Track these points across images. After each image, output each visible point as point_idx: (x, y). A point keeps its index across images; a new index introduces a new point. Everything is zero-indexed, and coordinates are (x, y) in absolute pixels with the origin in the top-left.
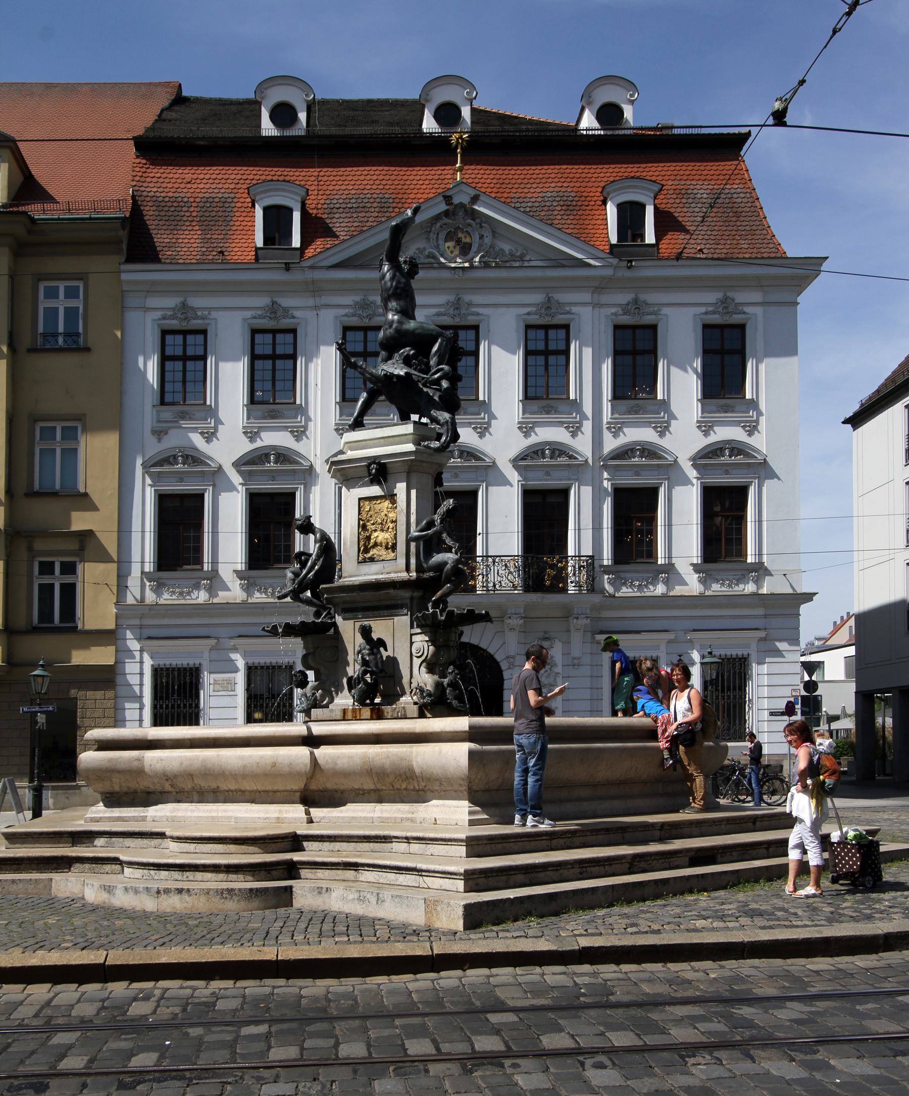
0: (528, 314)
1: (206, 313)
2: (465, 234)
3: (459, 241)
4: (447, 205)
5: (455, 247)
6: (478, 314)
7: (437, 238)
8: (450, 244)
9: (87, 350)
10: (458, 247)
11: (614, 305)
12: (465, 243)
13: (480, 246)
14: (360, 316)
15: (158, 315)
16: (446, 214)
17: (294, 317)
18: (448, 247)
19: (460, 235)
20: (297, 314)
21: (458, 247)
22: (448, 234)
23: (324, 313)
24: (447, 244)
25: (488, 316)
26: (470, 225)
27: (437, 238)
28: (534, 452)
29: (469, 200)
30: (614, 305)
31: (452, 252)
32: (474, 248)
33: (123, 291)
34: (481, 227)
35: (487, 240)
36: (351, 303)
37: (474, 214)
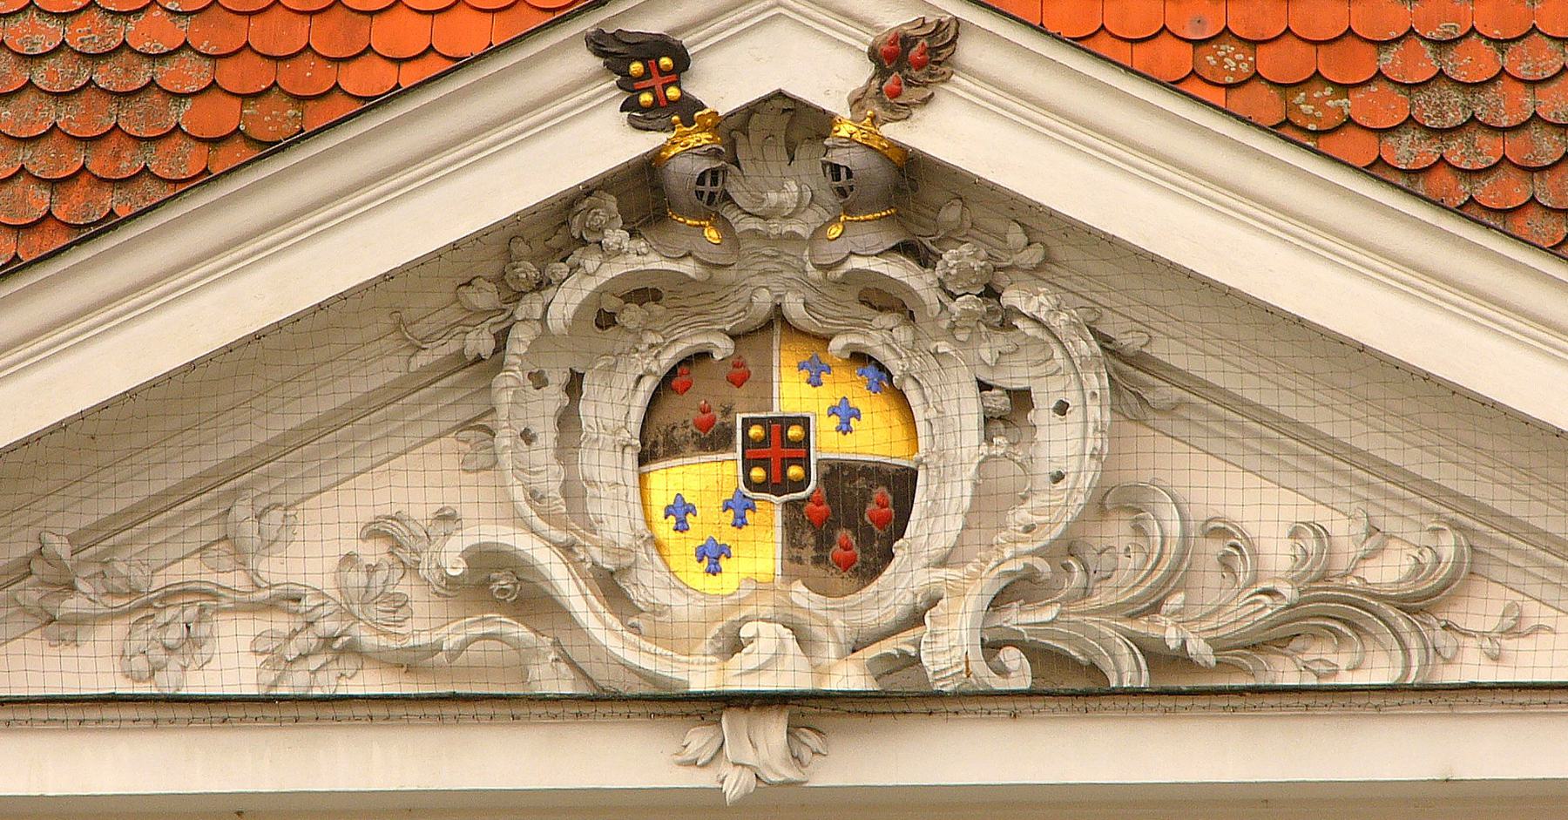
4: (640, 116)
5: (739, 510)
7: (567, 420)
8: (704, 479)
13: (988, 502)
16: (642, 194)
18: (680, 512)
19: (791, 393)
24: (673, 479)
26: (882, 299)
27: (567, 420)
29: (860, 73)
31: (713, 556)
32: (934, 522)
35: (1065, 443)
37: (913, 195)
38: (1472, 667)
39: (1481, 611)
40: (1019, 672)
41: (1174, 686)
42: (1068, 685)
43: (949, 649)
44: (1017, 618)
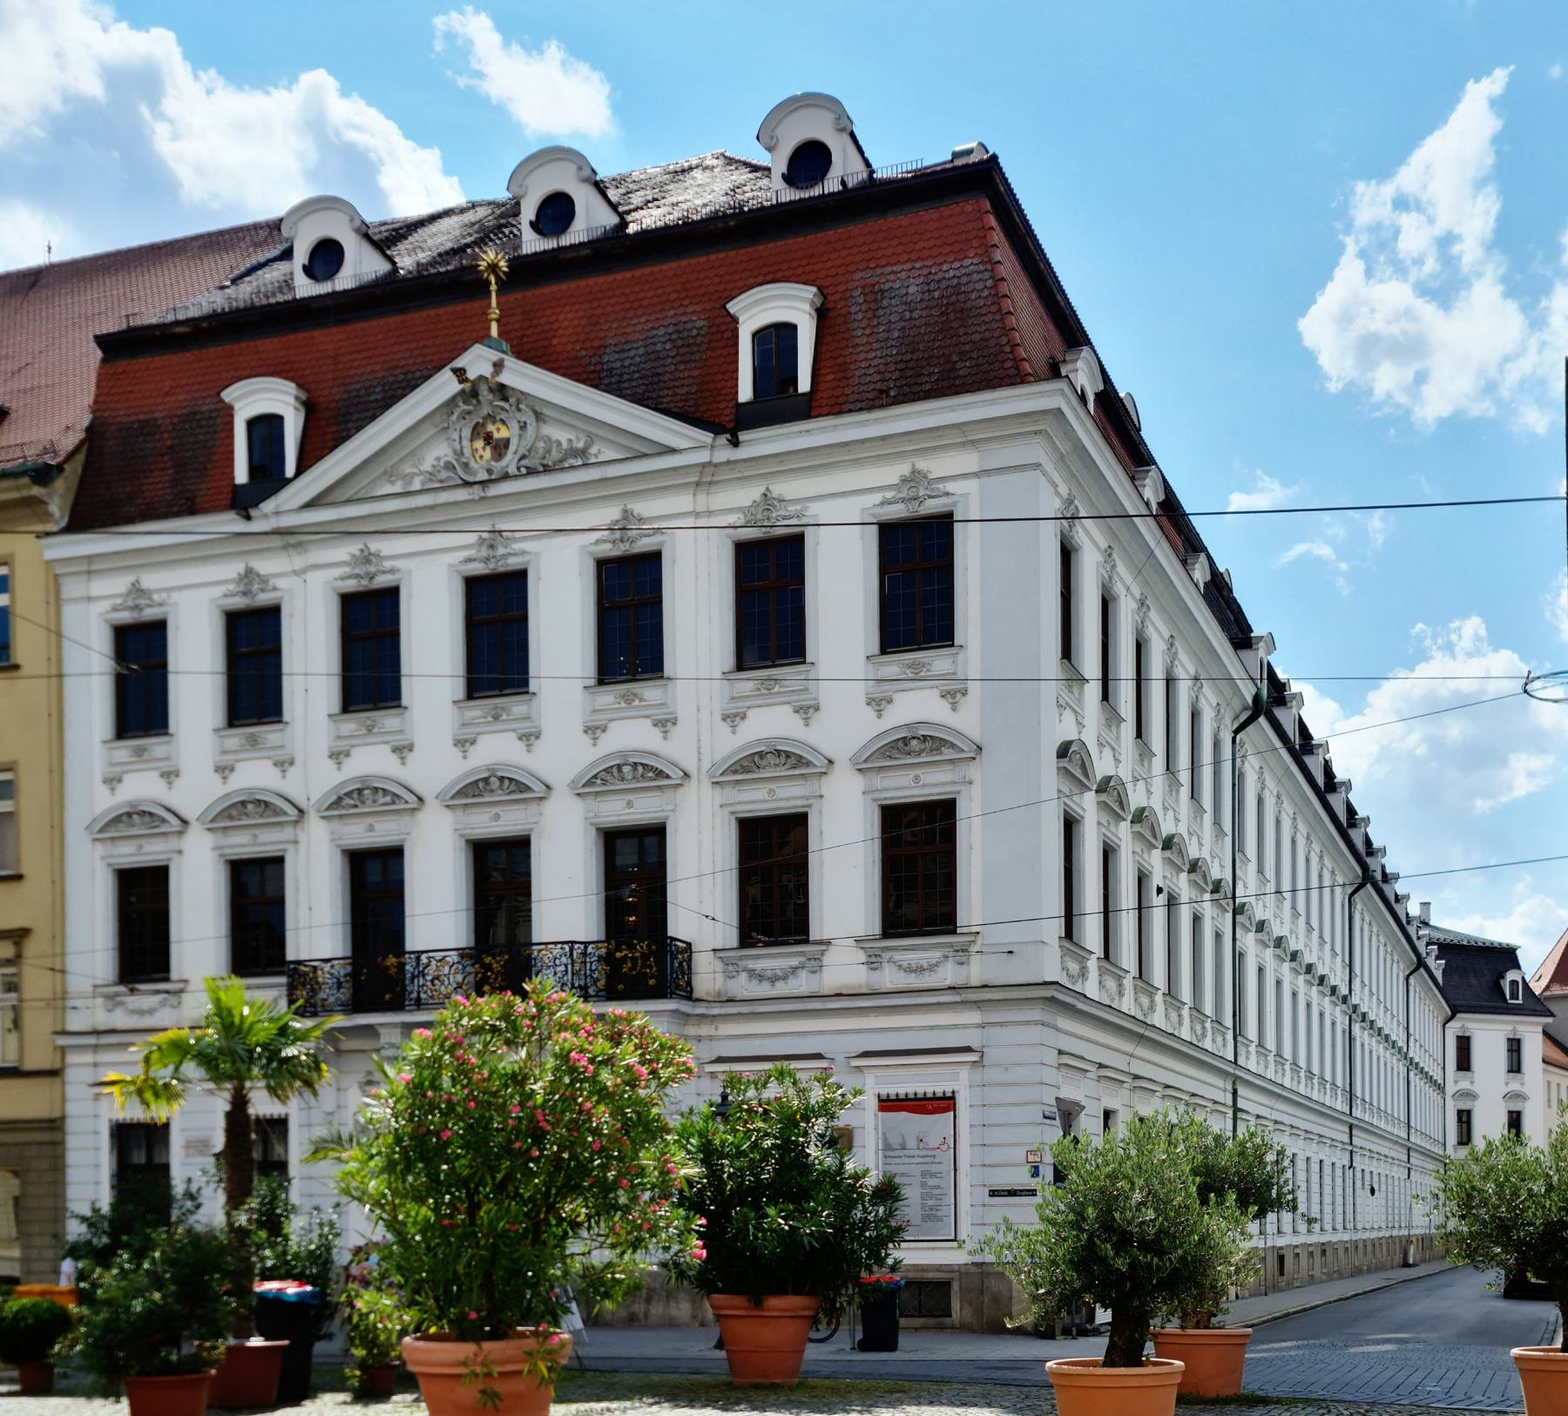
0: (597, 542)
1: (164, 595)
2: (499, 425)
3: (488, 438)
6: (523, 553)
9: (17, 667)
10: (488, 449)
11: (731, 511)
12: (499, 440)
14: (357, 576)
15: (105, 605)
17: (275, 589)
20: (281, 583)
21: (488, 449)
22: (474, 428)
23: (310, 576)
25: (538, 554)
28: (606, 770)
30: (731, 511)
33: (56, 576)
34: (519, 410)
36: (347, 558)
38: (593, 460)
39: (593, 450)
40: (524, 471)
41: (547, 469)
42: (531, 472)
43: (512, 470)
44: (523, 462)
